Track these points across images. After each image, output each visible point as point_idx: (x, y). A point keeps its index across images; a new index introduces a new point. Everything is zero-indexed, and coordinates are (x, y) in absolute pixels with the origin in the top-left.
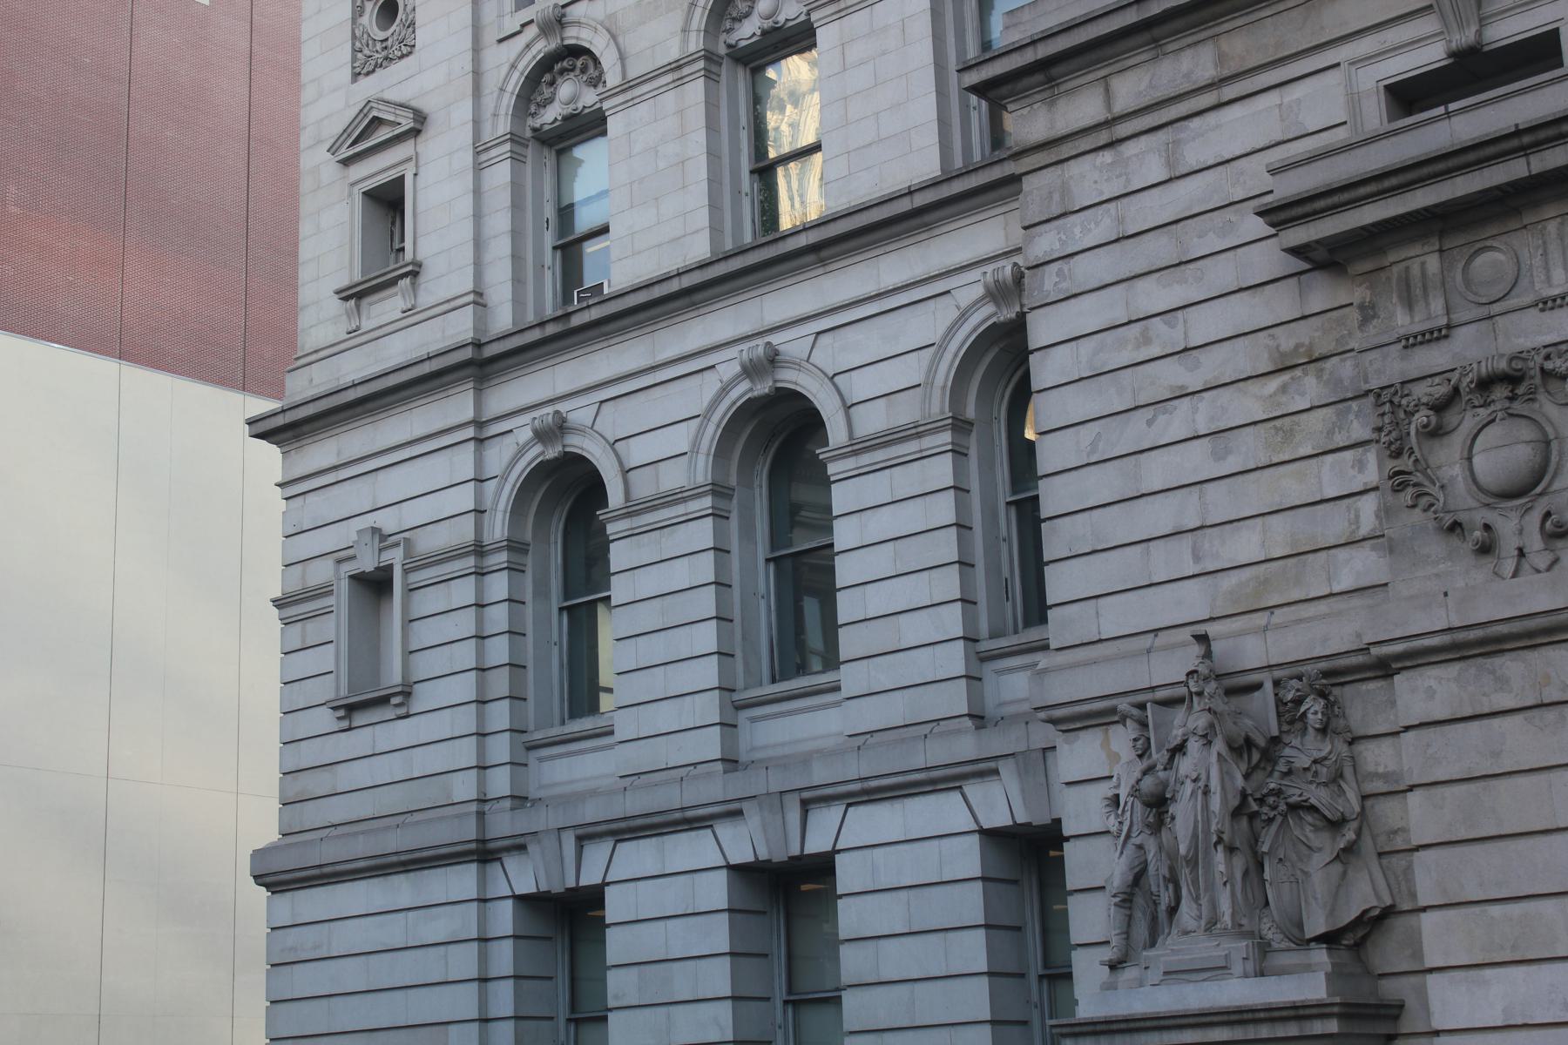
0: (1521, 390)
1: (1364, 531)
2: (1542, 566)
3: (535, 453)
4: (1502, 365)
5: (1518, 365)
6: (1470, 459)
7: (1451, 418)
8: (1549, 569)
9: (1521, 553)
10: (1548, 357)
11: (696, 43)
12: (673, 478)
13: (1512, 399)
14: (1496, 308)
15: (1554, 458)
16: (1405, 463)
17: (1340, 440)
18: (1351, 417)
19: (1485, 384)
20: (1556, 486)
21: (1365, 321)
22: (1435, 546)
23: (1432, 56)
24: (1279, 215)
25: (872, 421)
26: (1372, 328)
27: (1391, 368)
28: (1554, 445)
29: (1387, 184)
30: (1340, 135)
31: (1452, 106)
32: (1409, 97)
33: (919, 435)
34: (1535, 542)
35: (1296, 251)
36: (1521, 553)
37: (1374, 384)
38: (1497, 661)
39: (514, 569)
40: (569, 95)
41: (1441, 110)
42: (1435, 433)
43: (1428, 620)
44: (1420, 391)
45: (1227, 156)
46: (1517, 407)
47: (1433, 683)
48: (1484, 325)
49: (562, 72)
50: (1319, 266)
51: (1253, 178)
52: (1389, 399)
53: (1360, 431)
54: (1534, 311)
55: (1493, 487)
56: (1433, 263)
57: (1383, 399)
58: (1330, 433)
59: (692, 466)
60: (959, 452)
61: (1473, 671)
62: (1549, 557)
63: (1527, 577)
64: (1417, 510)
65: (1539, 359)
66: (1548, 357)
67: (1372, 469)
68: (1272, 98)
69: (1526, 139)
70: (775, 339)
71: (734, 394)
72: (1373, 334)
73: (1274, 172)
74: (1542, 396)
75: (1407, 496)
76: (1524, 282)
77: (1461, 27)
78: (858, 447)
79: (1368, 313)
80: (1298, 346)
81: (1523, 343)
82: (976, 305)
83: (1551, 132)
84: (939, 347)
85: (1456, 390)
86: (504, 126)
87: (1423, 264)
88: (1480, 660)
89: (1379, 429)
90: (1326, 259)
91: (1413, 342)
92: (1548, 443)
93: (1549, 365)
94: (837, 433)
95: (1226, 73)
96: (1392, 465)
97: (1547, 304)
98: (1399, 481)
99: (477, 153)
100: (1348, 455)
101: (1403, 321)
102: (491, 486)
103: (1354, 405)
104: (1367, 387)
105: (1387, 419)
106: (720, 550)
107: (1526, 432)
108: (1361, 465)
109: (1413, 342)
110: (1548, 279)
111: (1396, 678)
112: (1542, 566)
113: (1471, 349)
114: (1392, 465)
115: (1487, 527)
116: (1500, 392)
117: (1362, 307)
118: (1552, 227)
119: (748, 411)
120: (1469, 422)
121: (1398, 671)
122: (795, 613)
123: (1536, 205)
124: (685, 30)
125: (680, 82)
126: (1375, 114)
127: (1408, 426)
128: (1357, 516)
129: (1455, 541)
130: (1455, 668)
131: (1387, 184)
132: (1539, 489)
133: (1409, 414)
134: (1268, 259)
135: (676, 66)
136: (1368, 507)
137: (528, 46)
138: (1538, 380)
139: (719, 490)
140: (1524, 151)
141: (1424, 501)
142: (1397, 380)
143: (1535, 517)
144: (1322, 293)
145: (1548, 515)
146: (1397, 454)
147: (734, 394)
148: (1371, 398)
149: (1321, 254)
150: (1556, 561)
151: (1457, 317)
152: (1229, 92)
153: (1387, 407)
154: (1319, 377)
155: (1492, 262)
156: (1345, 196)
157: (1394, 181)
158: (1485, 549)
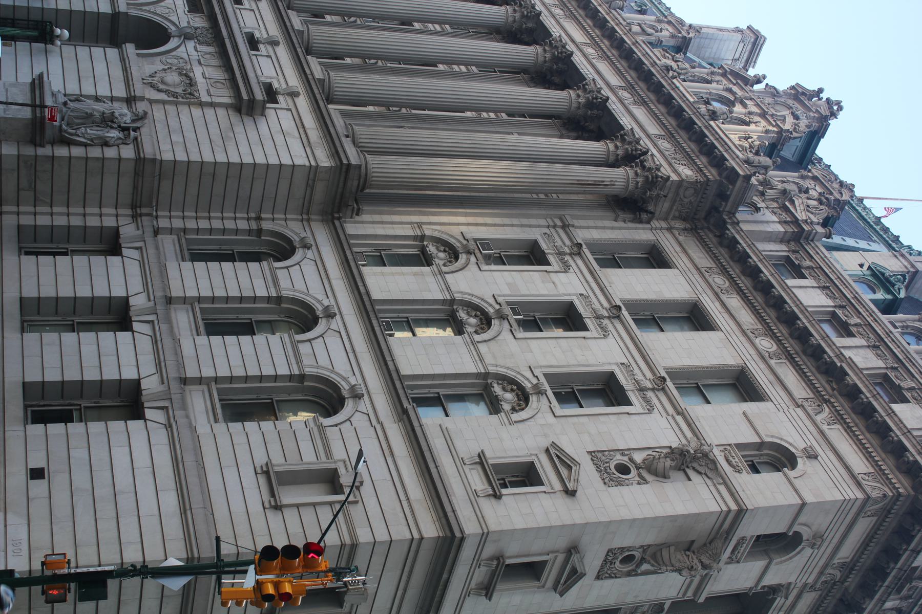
3: (296, 239)
11: (457, 296)
12: (284, 283)
25: (304, 349)
33: (297, 363)
39: (250, 232)
40: (441, 256)
49: (449, 254)
59: (312, 367)
60: (291, 377)
70: (338, 317)
71: (343, 383)
78: (295, 345)
82: (348, 383)
84: (333, 371)
86: (428, 232)
94: (326, 422)
99: (417, 223)
102: (283, 223)
106: (276, 378)
119: (335, 387)
122: (228, 320)
124: (462, 293)
125: (442, 291)
135: (448, 289)
137: (491, 305)
139: (302, 377)
147: (343, 383)
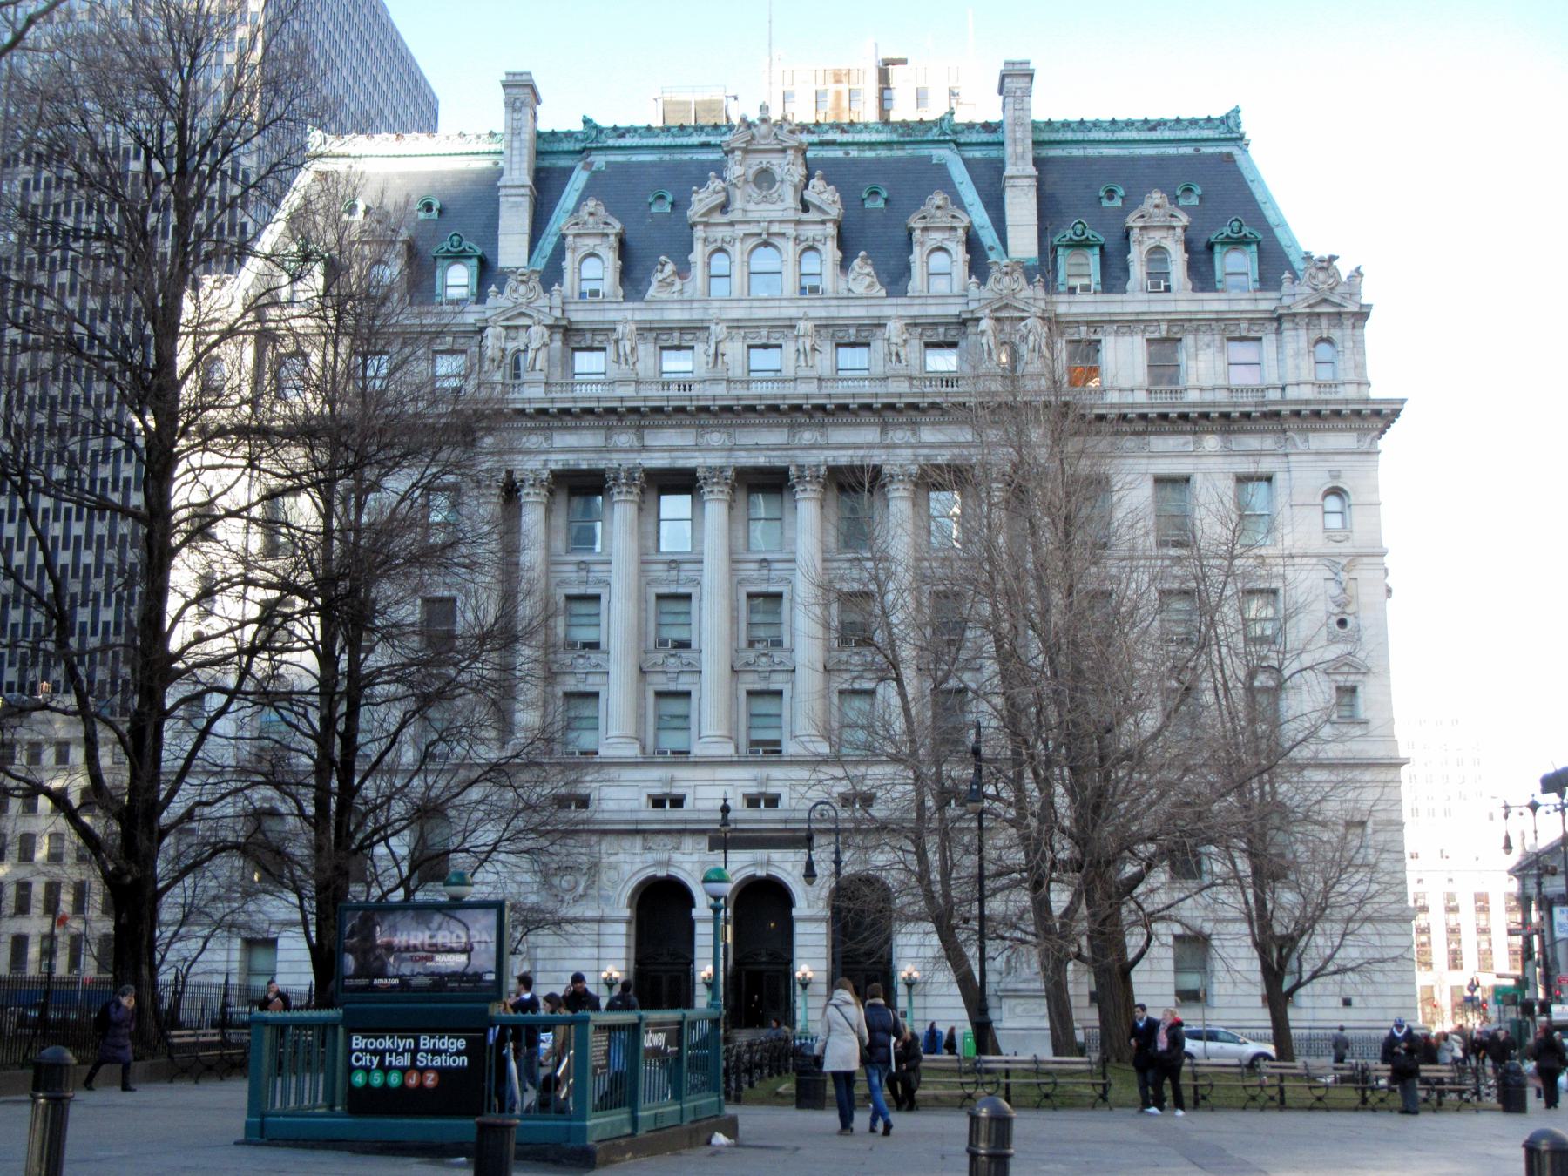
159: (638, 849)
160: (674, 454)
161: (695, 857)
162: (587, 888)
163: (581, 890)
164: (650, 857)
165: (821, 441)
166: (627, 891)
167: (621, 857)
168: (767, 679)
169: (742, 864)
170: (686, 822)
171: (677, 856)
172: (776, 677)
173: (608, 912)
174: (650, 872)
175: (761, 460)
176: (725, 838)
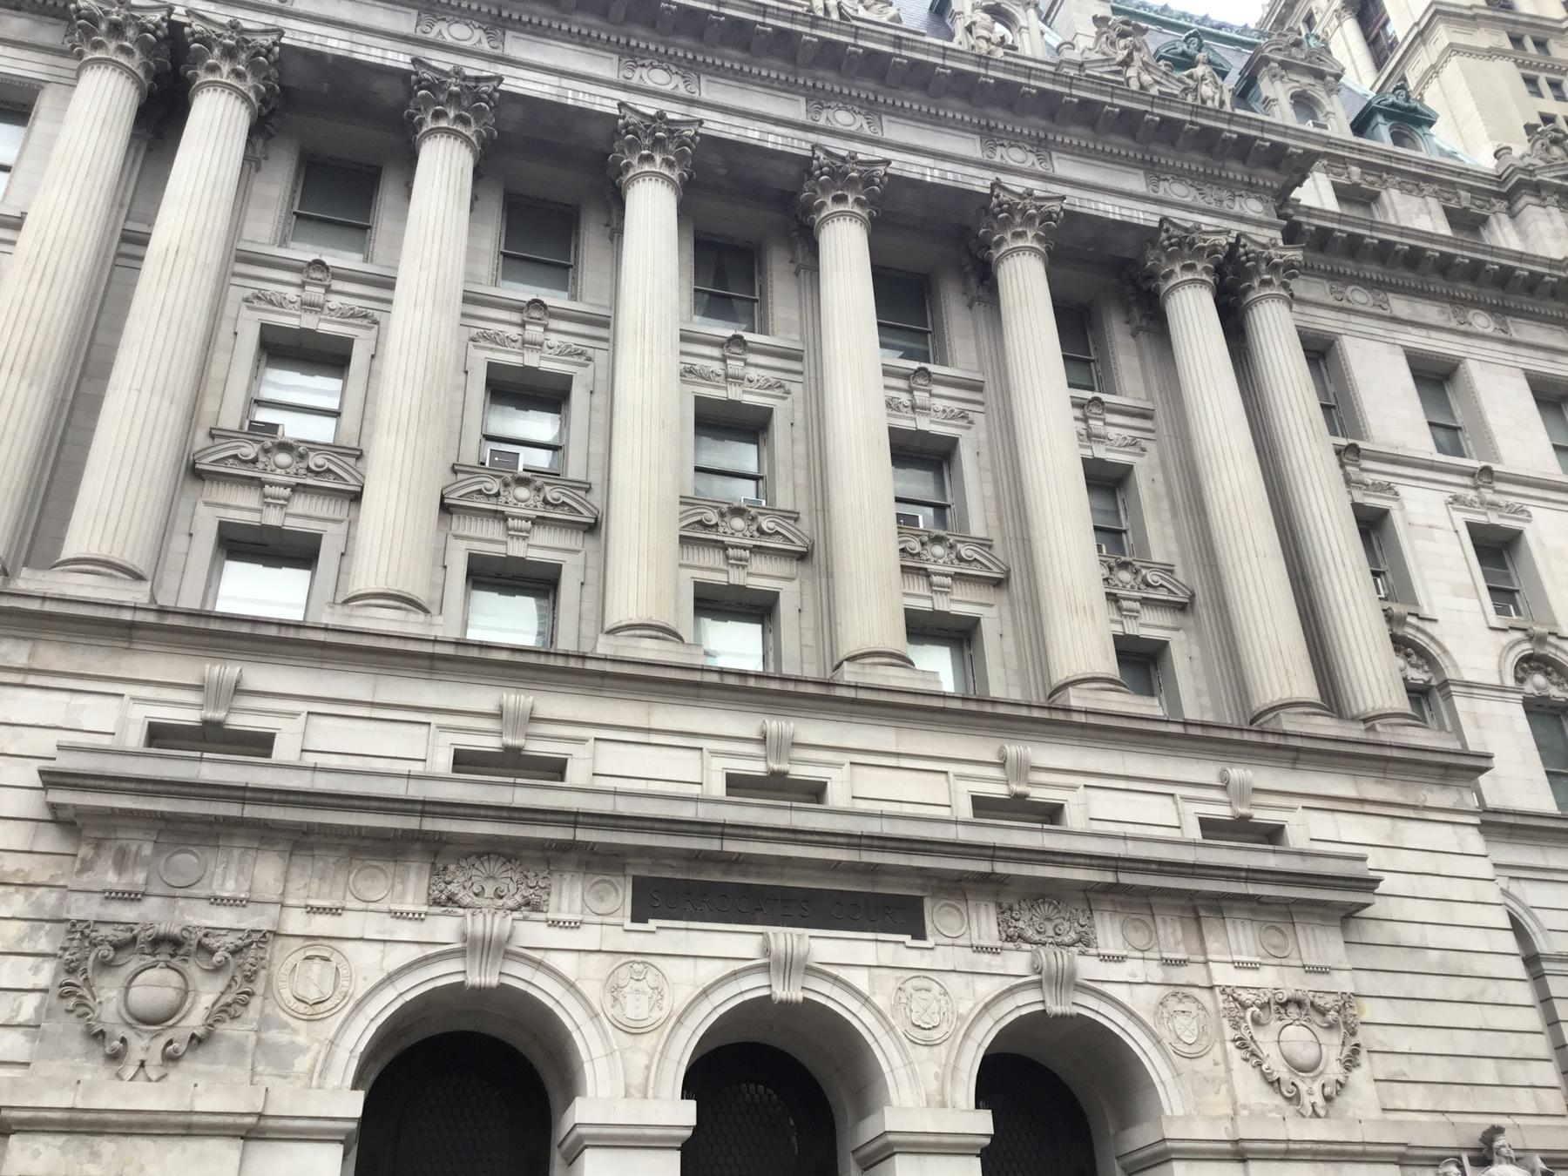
0: (181, 952)
1: (21, 1019)
2: (154, 1077)
4: (176, 931)
5: (185, 934)
6: (127, 988)
7: (122, 957)
8: (158, 1080)
9: (142, 1064)
10: (206, 935)
13: (172, 956)
14: (179, 892)
15: (187, 1005)
16: (77, 979)
17: (26, 947)
18: (42, 933)
19: (158, 942)
20: (183, 1023)
21: (81, 871)
22: (76, 1044)
23: (191, 717)
24: (52, 779)
26: (85, 877)
27: (85, 908)
28: (191, 995)
29: (143, 787)
30: (105, 741)
31: (206, 755)
32: (159, 735)
34: (155, 1057)
35: (53, 807)
36: (142, 1064)
37: (73, 916)
38: (98, 1139)
41: (198, 754)
42: (105, 965)
43: (57, 1098)
44: (105, 931)
45: (14, 721)
46: (175, 962)
47: (41, 1147)
48: (168, 901)
50: (56, 821)
51: (45, 743)
52: (81, 931)
53: (43, 945)
54: (206, 903)
55: (140, 1014)
56: (147, 849)
57: (79, 927)
58: (21, 940)
61: (76, 1143)
62: (162, 1071)
63: (140, 1083)
64: (73, 1016)
65: (200, 934)
66: (206, 935)
67: (45, 975)
68: (65, 697)
69: (248, 794)
72: (86, 880)
73: (60, 748)
74: (191, 960)
75: (72, 1001)
76: (205, 881)
77: (216, 708)
79: (86, 866)
80: (18, 871)
81: (192, 920)
83: (266, 796)
85: (134, 939)
87: (140, 847)
88: (84, 1137)
89: (65, 949)
90: (65, 821)
91: (112, 896)
92: (186, 992)
93: (206, 941)
95: (35, 666)
96: (63, 978)
97: (216, 901)
98: (67, 991)
100: (30, 960)
101: (111, 879)
103: (48, 926)
104: (65, 916)
105: (75, 943)
107: (174, 978)
108: (36, 970)
109: (112, 896)
110: (223, 884)
111: (13, 1138)
112: (154, 1077)
113: (154, 915)
114: (63, 978)
115: (123, 1040)
116: (166, 949)
117: (83, 860)
118: (236, 853)
120: (134, 964)
121: (15, 1132)
123: (231, 836)
126: (135, 738)
127: (87, 955)
128: (20, 1007)
129: (94, 1045)
130: (60, 1140)
131: (143, 787)
132: (170, 1022)
133: (94, 945)
134: (30, 804)
136: (30, 1003)
138: (193, 948)
140: (244, 801)
141: (81, 1010)
142: (92, 918)
143: (162, 1041)
144: (50, 840)
145: (170, 1042)
146: (71, 971)
148: (69, 925)
149: (62, 814)
150: (164, 1076)
151: (151, 890)
152: (32, 680)
153: (78, 935)
154: (27, 898)
155: (186, 861)
156: (112, 784)
157: (150, 787)
158: (115, 1057)
159: (413, 901)
160: (565, 82)
161: (588, 937)
162: (224, 1012)
163: (195, 1020)
164: (445, 929)
165: (867, 131)
166: (360, 1034)
167: (349, 924)
168: (741, 564)
169: (710, 968)
170: (574, 819)
171: (532, 933)
172: (759, 564)
173: (288, 1101)
174: (445, 974)
175: (752, 133)
176: (682, 879)
